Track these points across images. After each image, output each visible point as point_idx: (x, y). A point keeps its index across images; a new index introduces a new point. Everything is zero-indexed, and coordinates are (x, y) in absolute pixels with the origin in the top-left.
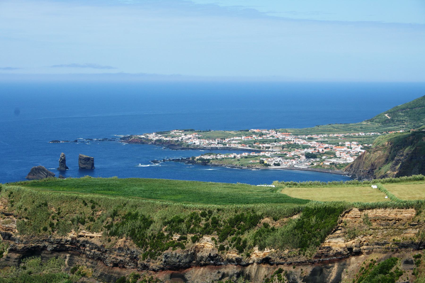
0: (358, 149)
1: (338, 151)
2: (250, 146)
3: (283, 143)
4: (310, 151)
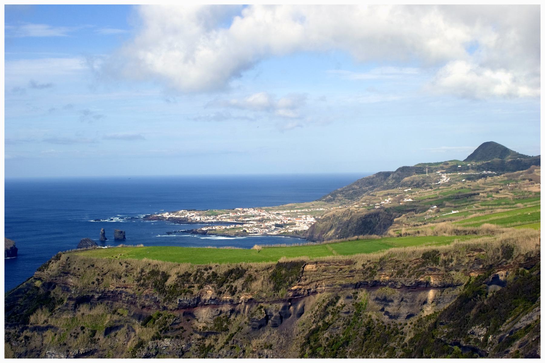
0: (311, 220)
1: (297, 222)
2: (236, 221)
3: (258, 218)
4: (278, 222)
